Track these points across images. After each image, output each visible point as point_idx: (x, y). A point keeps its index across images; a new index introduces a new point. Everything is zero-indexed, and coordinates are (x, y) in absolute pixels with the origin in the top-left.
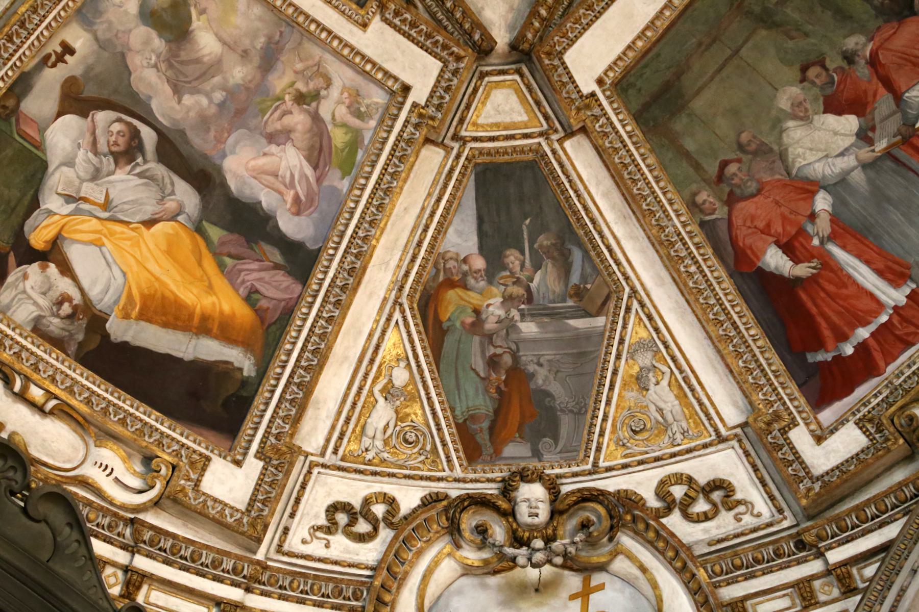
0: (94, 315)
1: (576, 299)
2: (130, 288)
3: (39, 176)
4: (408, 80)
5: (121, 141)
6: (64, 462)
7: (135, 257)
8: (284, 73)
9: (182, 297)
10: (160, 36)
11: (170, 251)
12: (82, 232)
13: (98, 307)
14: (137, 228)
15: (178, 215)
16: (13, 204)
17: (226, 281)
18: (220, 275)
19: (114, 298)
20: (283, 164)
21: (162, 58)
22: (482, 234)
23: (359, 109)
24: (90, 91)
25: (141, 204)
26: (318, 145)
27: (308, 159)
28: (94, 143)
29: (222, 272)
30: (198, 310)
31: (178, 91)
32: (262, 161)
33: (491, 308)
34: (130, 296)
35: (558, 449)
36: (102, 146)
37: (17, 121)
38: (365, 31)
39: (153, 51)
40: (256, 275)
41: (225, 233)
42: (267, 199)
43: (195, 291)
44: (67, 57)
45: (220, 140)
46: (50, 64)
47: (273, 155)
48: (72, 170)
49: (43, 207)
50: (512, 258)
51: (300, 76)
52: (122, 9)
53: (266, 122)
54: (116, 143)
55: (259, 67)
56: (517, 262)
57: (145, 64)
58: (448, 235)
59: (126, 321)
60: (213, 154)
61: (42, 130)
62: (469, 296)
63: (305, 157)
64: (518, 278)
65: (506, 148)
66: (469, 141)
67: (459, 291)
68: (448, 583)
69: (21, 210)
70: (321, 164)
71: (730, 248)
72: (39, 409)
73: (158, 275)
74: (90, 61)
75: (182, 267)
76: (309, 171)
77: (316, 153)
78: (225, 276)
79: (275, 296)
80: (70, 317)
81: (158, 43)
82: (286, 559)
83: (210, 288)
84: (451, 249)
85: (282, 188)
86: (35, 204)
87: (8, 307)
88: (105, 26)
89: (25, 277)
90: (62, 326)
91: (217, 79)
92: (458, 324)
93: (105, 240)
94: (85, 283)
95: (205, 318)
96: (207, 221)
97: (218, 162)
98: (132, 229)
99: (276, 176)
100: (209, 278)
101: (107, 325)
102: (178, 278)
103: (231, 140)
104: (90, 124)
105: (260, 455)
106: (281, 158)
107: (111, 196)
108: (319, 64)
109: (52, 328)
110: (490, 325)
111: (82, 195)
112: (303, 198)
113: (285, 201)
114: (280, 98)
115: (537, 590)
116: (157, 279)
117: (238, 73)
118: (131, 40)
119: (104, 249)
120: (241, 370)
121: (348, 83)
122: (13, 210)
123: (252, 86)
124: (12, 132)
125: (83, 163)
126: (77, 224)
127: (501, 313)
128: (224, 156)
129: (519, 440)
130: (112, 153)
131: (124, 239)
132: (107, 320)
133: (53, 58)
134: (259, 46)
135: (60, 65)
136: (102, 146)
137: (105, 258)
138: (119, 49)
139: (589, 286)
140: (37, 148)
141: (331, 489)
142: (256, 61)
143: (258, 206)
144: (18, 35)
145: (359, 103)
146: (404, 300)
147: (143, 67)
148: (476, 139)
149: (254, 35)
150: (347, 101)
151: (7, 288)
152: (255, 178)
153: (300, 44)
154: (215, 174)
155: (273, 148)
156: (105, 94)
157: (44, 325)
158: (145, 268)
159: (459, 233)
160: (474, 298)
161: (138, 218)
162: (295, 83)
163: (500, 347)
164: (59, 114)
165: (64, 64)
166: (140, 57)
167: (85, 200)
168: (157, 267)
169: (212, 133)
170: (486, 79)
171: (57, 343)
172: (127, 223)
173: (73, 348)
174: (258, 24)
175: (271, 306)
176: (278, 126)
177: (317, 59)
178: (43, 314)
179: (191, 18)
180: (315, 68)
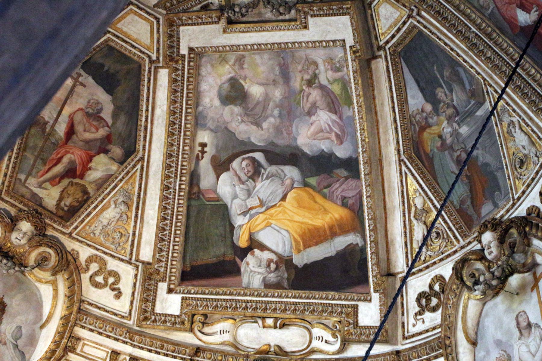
0: (286, 260)
1: (473, 98)
2: (293, 236)
3: (226, 213)
4: (342, 38)
5: (250, 168)
6: (302, 346)
7: (288, 220)
8: (296, 77)
9: (317, 224)
10: (236, 105)
11: (300, 205)
12: (259, 225)
13: (285, 255)
14: (280, 205)
15: (293, 185)
16: (223, 235)
17: (330, 202)
18: (326, 201)
19: (289, 246)
20: (322, 122)
21: (243, 115)
22: (422, 90)
23: (336, 66)
24: (224, 156)
25: (275, 192)
26: (330, 100)
27: (330, 111)
28: (240, 179)
29: (326, 198)
30: (326, 226)
31: (258, 124)
32: (312, 129)
33: (445, 130)
34: (296, 241)
35: (503, 197)
36: (244, 178)
37: (203, 196)
38: (308, 29)
39: (237, 115)
40: (340, 189)
41: (317, 177)
42: (325, 146)
43: (320, 217)
44: (206, 149)
45: (289, 133)
46: (200, 158)
47: (315, 121)
48: (238, 199)
49: (236, 226)
50: (440, 94)
51: (303, 72)
52: (213, 107)
53: (303, 107)
54: (248, 171)
55: (284, 83)
56: (443, 94)
57: (237, 124)
58: (409, 102)
59: (300, 254)
60: (291, 142)
61: (215, 191)
62: (433, 130)
63: (328, 111)
64: (448, 103)
65: (402, 35)
66: (386, 45)
67: (428, 130)
68: (478, 313)
69: (228, 234)
70: (337, 110)
71: (505, 23)
73: (301, 221)
74: (215, 143)
75: (309, 209)
76: (334, 117)
77: (332, 106)
78: (328, 200)
79: (353, 195)
80: (277, 269)
81: (237, 109)
82: (408, 341)
83: (326, 211)
84: (414, 109)
85: (327, 135)
86: (232, 227)
87: (249, 283)
88: (211, 122)
89: (248, 264)
90: (275, 275)
91: (271, 104)
92: (435, 150)
93: (270, 221)
94: (274, 248)
95: (331, 228)
96: (307, 178)
97: (295, 145)
98: (279, 207)
99: (322, 131)
100: (322, 206)
101: (294, 261)
102: (310, 216)
103: (294, 128)
104: (233, 172)
105: (376, 291)
106: (319, 120)
107: (261, 198)
108: (307, 59)
109: (272, 280)
110: (449, 141)
111: (249, 207)
112: (339, 133)
113: (333, 141)
114: (302, 91)
115: (517, 294)
116: (302, 223)
117: (277, 94)
118: (225, 118)
119: (272, 225)
120: (357, 244)
121: (324, 58)
122: (225, 237)
123: (286, 95)
124: (203, 202)
125: (241, 192)
126: (255, 222)
127: (450, 129)
128: (296, 139)
129: (486, 201)
130: (250, 177)
131: (277, 214)
132: (292, 259)
133: (200, 155)
134: (278, 74)
135: (205, 155)
136: (244, 178)
137: (275, 229)
138: (223, 127)
139: (474, 87)
140: (218, 201)
141: (415, 288)
142: (281, 81)
143: (323, 153)
144: (172, 162)
145: (334, 64)
146: (403, 157)
147: (237, 126)
148: (387, 42)
149: (273, 69)
150: (329, 67)
151: (243, 274)
152: (314, 139)
153: (293, 56)
154: (297, 152)
155: (314, 118)
156: (230, 153)
157: (268, 281)
158: (295, 221)
159: (413, 97)
160: (435, 129)
161: (278, 199)
162: (303, 77)
163: (458, 150)
164: (218, 178)
165: (206, 154)
166: (234, 123)
167: (251, 208)
168: (299, 217)
169: (285, 133)
170: (372, 6)
171: (277, 286)
172: (275, 206)
173: (285, 284)
174: (271, 62)
175: (354, 201)
176: (309, 105)
177: (304, 57)
178: (265, 276)
179: (243, 86)
180: (307, 62)
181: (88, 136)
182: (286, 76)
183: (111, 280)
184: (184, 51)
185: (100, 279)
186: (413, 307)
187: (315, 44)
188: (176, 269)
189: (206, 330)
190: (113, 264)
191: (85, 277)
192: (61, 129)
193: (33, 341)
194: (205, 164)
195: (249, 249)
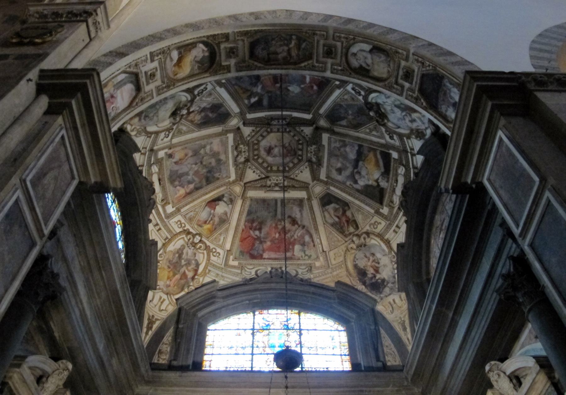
31: (348, 168)
42: (355, 152)
72: (397, 183)
76: (348, 146)
80: (384, 177)
81: (343, 172)
117: (341, 159)
171: (388, 178)
181: (341, 213)
182: (337, 156)
183: (376, 224)
184: (326, 180)
185: (375, 226)
186: (392, 142)
187: (329, 144)
188: (378, 205)
189: (395, 202)
190: (373, 221)
191: (374, 230)
192: (337, 219)
193: (384, 250)
194: (355, 186)
195: (378, 183)
